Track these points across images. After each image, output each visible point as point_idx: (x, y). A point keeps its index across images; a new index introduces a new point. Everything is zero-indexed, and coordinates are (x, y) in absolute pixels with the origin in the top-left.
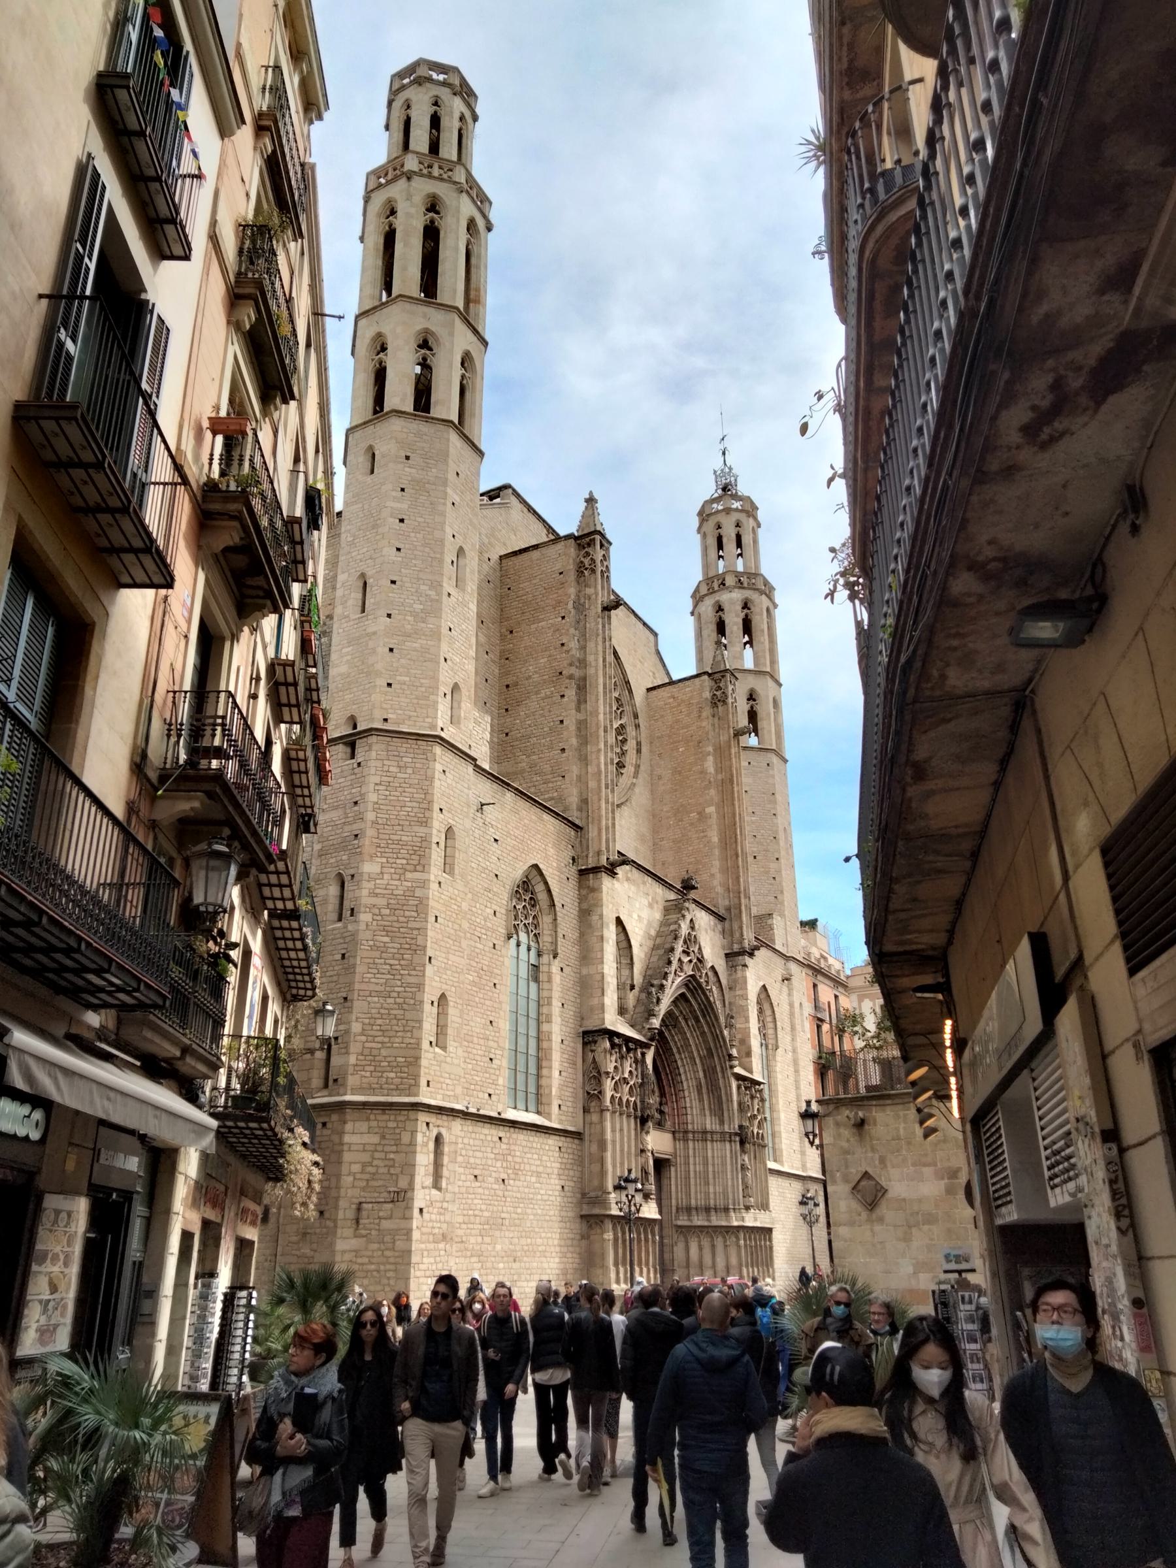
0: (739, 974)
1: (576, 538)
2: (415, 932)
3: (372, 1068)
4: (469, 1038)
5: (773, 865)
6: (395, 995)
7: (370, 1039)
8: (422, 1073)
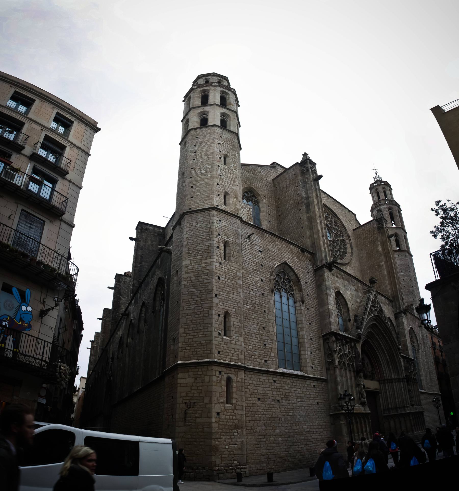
3: (189, 348)
6: (199, 313)
7: (188, 334)
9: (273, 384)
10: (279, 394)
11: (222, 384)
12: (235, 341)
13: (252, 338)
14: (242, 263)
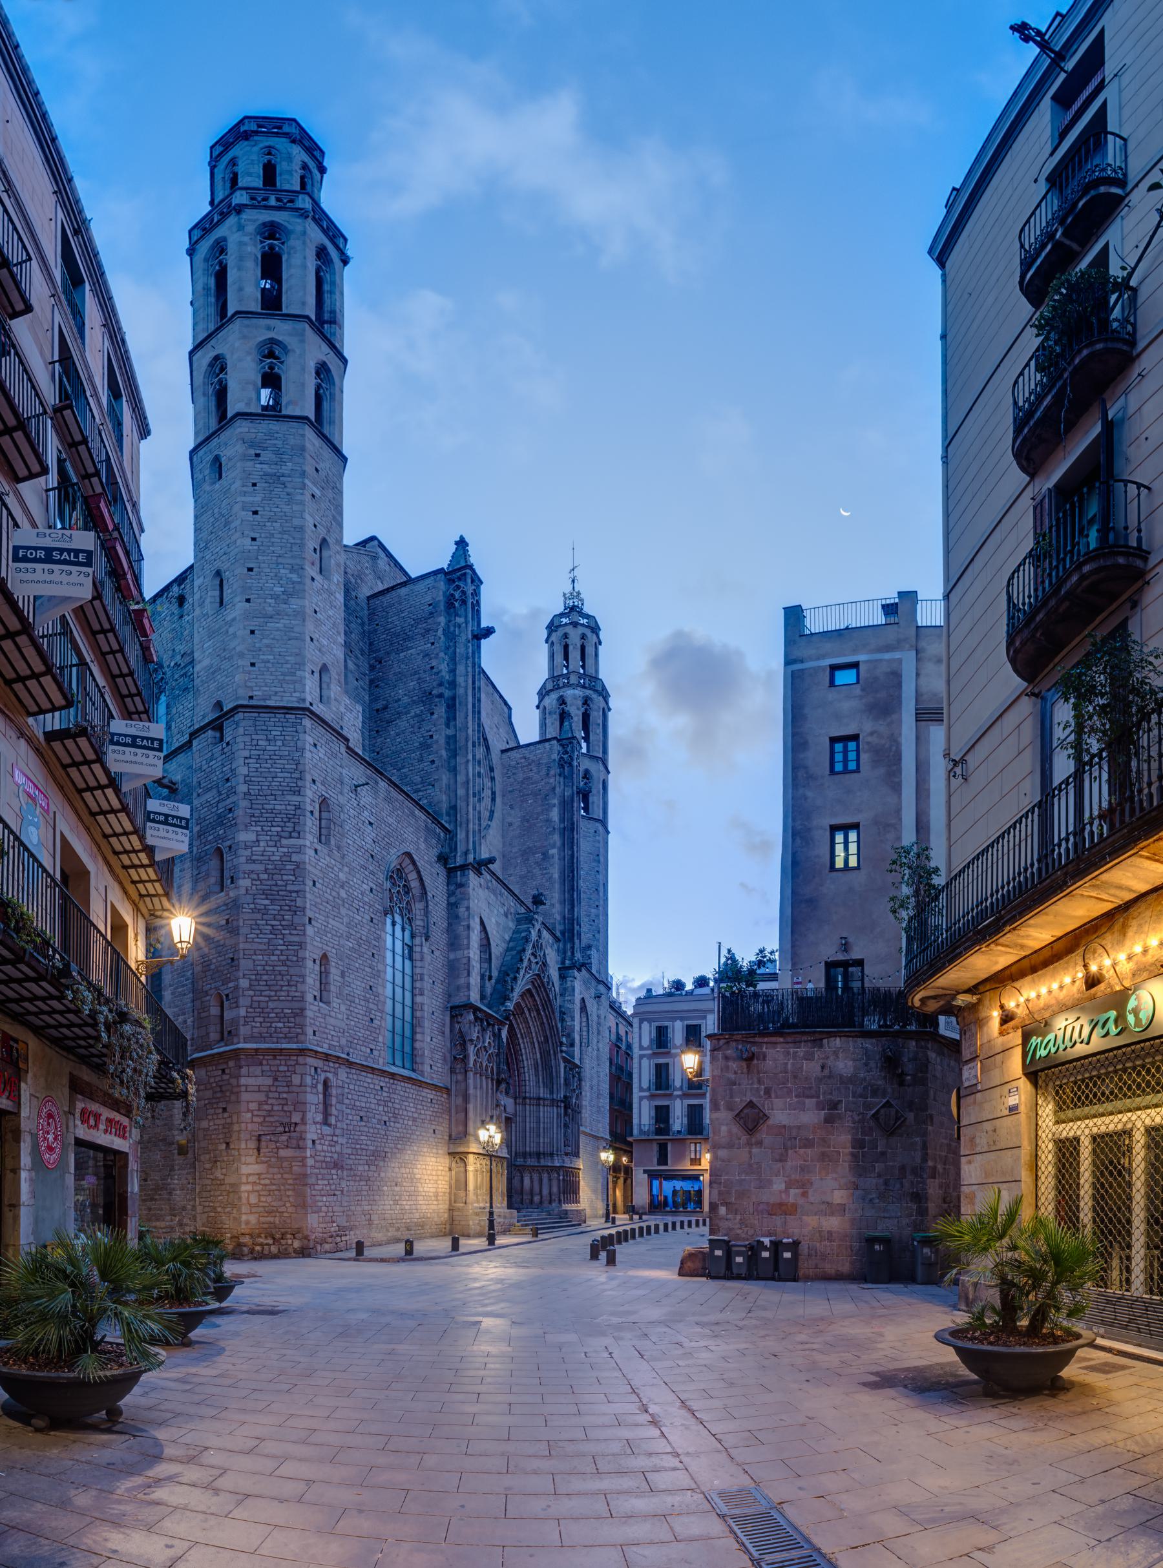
2: (294, 895)
6: (278, 952)
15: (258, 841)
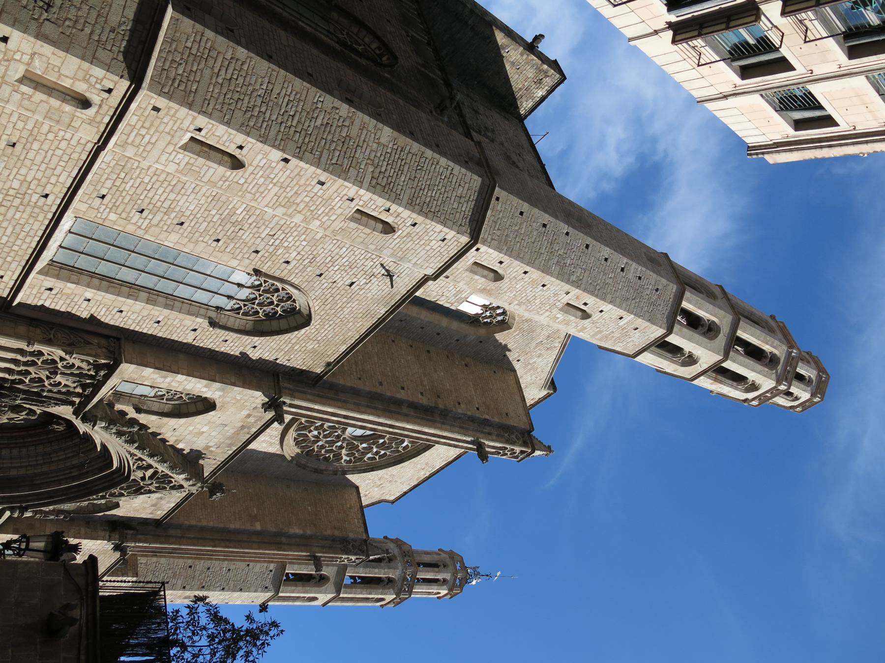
0: (101, 533)
1: (529, 432)
3: (194, 52)
4: (176, 190)
5: (180, 582)
8: (172, 104)
9: (39, 189)
10: (9, 193)
11: (77, 83)
12: (170, 154)
13: (167, 191)
14: (338, 240)
15: (379, 143)
